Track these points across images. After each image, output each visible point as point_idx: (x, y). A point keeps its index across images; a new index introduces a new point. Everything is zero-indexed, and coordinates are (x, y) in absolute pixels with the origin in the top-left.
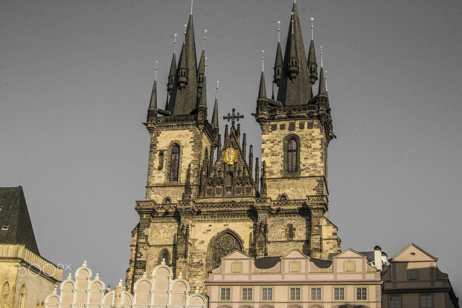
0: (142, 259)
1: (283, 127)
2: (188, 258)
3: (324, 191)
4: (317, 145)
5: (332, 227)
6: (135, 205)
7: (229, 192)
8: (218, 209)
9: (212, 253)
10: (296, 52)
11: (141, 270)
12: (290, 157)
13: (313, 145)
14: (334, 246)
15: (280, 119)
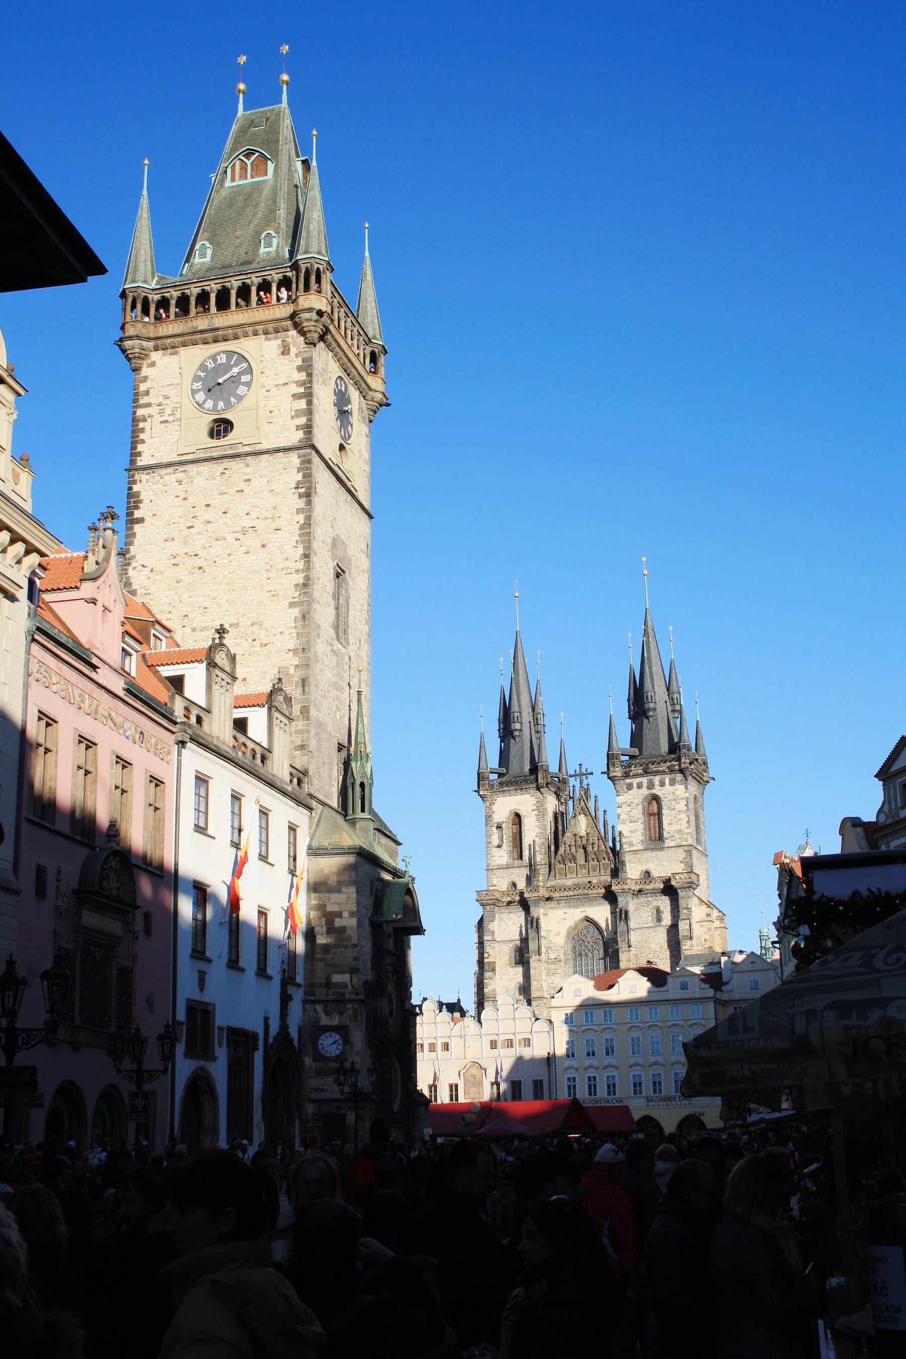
0: (490, 960)
1: (640, 786)
2: (543, 956)
3: (695, 861)
4: (682, 805)
5: (705, 906)
6: (475, 896)
7: (584, 871)
8: (571, 893)
9: (570, 945)
10: (652, 679)
11: (491, 973)
12: (652, 822)
13: (677, 806)
14: (709, 929)
15: (636, 776)
